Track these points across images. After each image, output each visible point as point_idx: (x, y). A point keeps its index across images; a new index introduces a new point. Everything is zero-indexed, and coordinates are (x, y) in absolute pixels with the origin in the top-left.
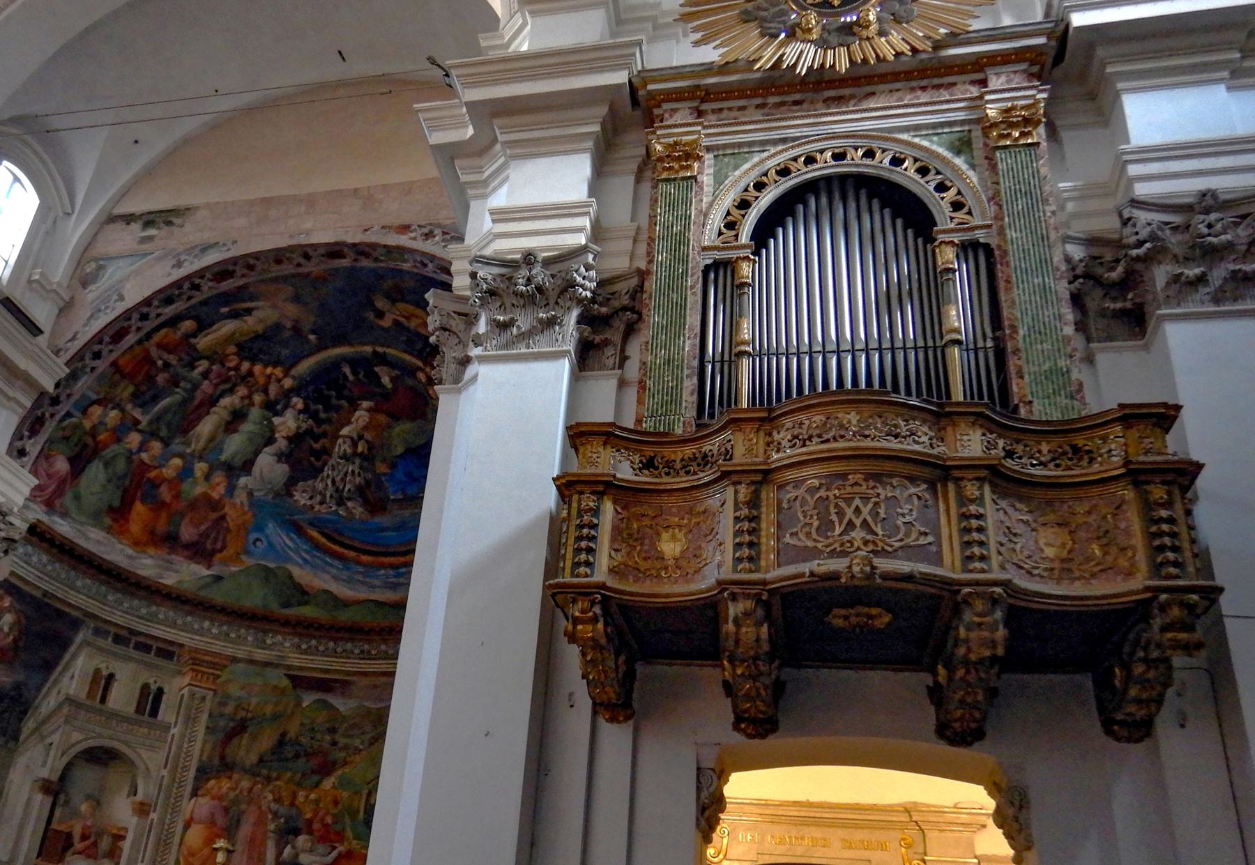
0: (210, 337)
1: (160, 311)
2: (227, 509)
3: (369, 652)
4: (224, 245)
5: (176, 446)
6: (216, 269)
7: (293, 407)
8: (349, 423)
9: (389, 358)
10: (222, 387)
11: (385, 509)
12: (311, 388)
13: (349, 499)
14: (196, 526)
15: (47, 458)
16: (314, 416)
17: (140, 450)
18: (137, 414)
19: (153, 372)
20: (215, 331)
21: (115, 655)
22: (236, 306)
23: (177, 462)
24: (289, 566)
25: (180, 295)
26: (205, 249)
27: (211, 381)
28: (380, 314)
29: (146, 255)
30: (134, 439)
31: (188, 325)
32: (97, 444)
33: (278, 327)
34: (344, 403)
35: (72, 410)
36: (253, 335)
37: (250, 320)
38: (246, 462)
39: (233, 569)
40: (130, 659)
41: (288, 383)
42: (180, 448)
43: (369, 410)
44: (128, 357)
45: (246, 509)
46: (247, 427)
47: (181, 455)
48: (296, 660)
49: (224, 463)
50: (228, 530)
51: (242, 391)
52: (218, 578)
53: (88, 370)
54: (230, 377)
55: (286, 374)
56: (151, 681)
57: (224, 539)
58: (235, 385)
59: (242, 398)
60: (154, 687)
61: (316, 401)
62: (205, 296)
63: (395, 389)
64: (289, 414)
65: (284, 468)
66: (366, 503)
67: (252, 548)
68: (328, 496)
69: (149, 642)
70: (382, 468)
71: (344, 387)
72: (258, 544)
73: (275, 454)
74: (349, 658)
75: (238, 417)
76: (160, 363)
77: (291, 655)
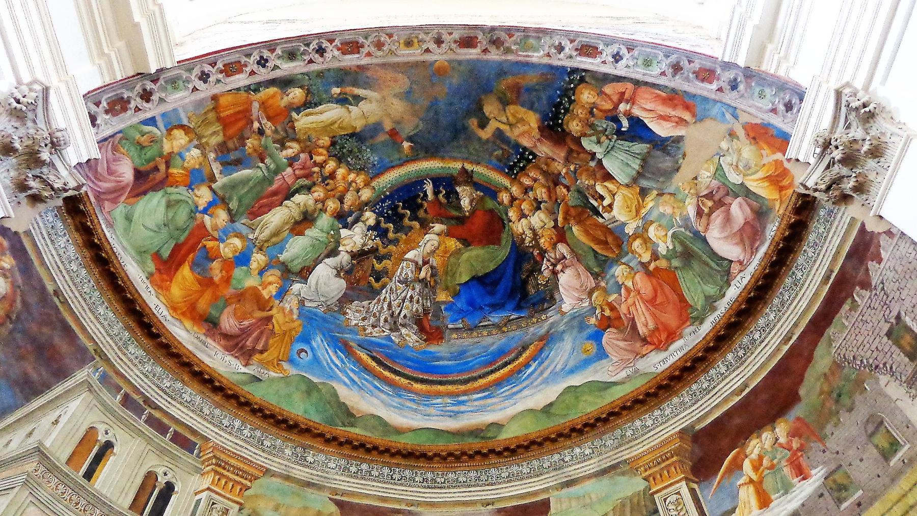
0: (311, 118)
1: (278, 63)
5: (241, 225)
6: (348, 37)
11: (442, 338)
12: (388, 203)
13: (404, 326)
14: (241, 319)
15: (115, 149)
16: (383, 234)
17: (205, 211)
18: (216, 168)
19: (247, 133)
21: (121, 420)
22: (348, 89)
23: (237, 242)
24: (335, 384)
25: (303, 54)
27: (294, 171)
30: (204, 195)
31: (296, 94)
32: (168, 175)
33: (375, 128)
34: (416, 224)
35: (159, 119)
38: (302, 269)
39: (273, 374)
40: (140, 433)
41: (366, 194)
42: (244, 230)
43: (438, 235)
45: (295, 317)
46: (312, 233)
51: (319, 193)
53: (191, 86)
55: (367, 184)
56: (160, 471)
58: (314, 184)
60: (162, 480)
61: (388, 219)
62: (325, 66)
63: (473, 212)
64: (359, 228)
65: (341, 284)
66: (422, 329)
67: (296, 357)
68: (382, 319)
69: (166, 421)
70: (442, 297)
72: (303, 355)
73: (335, 268)
75: (306, 219)
76: (256, 125)
77: (337, 477)
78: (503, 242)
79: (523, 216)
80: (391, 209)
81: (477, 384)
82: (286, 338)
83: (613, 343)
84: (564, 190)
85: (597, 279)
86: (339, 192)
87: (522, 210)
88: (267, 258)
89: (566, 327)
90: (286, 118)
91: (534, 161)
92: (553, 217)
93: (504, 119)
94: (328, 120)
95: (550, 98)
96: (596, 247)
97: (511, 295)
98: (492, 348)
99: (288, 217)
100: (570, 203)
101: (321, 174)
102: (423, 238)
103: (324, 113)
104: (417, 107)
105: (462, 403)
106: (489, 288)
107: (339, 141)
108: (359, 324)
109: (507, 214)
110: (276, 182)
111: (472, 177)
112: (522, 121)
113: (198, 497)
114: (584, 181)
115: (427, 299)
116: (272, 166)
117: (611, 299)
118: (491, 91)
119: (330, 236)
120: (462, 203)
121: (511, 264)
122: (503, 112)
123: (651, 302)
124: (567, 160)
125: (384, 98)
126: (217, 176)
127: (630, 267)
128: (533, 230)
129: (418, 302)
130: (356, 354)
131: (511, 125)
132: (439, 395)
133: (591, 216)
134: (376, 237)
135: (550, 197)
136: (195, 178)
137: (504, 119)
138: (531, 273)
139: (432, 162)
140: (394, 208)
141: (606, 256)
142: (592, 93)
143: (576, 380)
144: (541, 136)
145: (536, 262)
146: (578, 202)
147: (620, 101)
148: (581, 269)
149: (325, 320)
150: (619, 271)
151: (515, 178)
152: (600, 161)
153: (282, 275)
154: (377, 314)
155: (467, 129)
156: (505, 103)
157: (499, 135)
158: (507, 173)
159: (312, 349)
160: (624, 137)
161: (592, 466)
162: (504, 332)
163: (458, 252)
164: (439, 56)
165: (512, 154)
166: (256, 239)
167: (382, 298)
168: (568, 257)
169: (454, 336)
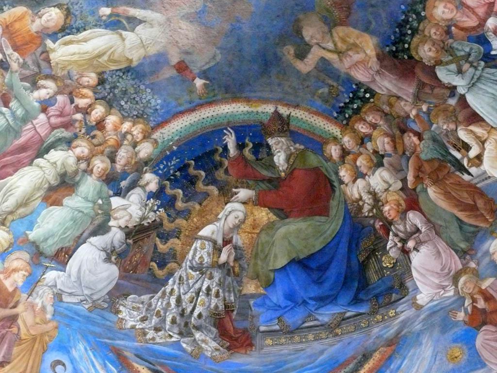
0: (73, 48)
2: (20, 309)
7: (143, 187)
9: (293, 125)
10: (62, 133)
11: (251, 345)
13: (198, 328)
16: (169, 203)
20: (78, 42)
22: (121, 9)
27: (49, 118)
34: (213, 190)
36: (123, 66)
41: (145, 150)
43: (244, 203)
45: (49, 316)
46: (75, 202)
49: (34, 244)
50: (18, 340)
51: (82, 148)
54: (76, 120)
55: (146, 137)
57: (10, 349)
58: (76, 137)
59: (79, 159)
61: (175, 182)
63: (291, 172)
64: (136, 196)
65: (112, 271)
68: (169, 319)
70: (251, 288)
71: (218, 166)
72: (59, 368)
73: (104, 250)
78: (333, 212)
79: (358, 175)
80: (180, 170)
82: (36, 346)
83: (492, 347)
84: (415, 139)
85: (465, 258)
86: (110, 146)
87: (357, 166)
88: (11, 236)
89: (423, 326)
90: (38, 47)
91: (372, 100)
92: (400, 176)
93: (330, 45)
94: (94, 50)
95: (391, 14)
96: (461, 215)
97: (346, 283)
98: (321, 358)
99: (40, 181)
100: (423, 156)
101: (86, 124)
102: (223, 209)
103: (90, 40)
104: (214, 32)
106: (315, 276)
107: (110, 79)
108: (137, 327)
109: (337, 173)
110: (25, 133)
111: (288, 124)
112: (355, 47)
114: (442, 125)
115: (229, 291)
116: (20, 112)
117: (486, 284)
118: (313, 9)
119: (97, 207)
120: (275, 158)
121: (345, 240)
122: (329, 36)
124: (418, 98)
125: (169, 20)
128: (374, 194)
129: (217, 295)
130: (133, 367)
131: (339, 53)
133: (453, 173)
134: (159, 207)
135: (395, 148)
137: (330, 45)
138: (374, 251)
139: (234, 105)
140: (184, 168)
141: (477, 227)
142: (449, 5)
144: (381, 67)
145: (379, 238)
146: (436, 155)
147: (489, 14)
148: (442, 245)
149: (88, 319)
151: (347, 124)
152: (462, 99)
153: (32, 258)
154: (162, 313)
155: (281, 59)
156: (331, 23)
157: (324, 67)
158: (336, 118)
159: (72, 361)
160: (493, 63)
162: (337, 335)
163: (270, 227)
165: (343, 93)
168: (423, 230)
169: (269, 342)
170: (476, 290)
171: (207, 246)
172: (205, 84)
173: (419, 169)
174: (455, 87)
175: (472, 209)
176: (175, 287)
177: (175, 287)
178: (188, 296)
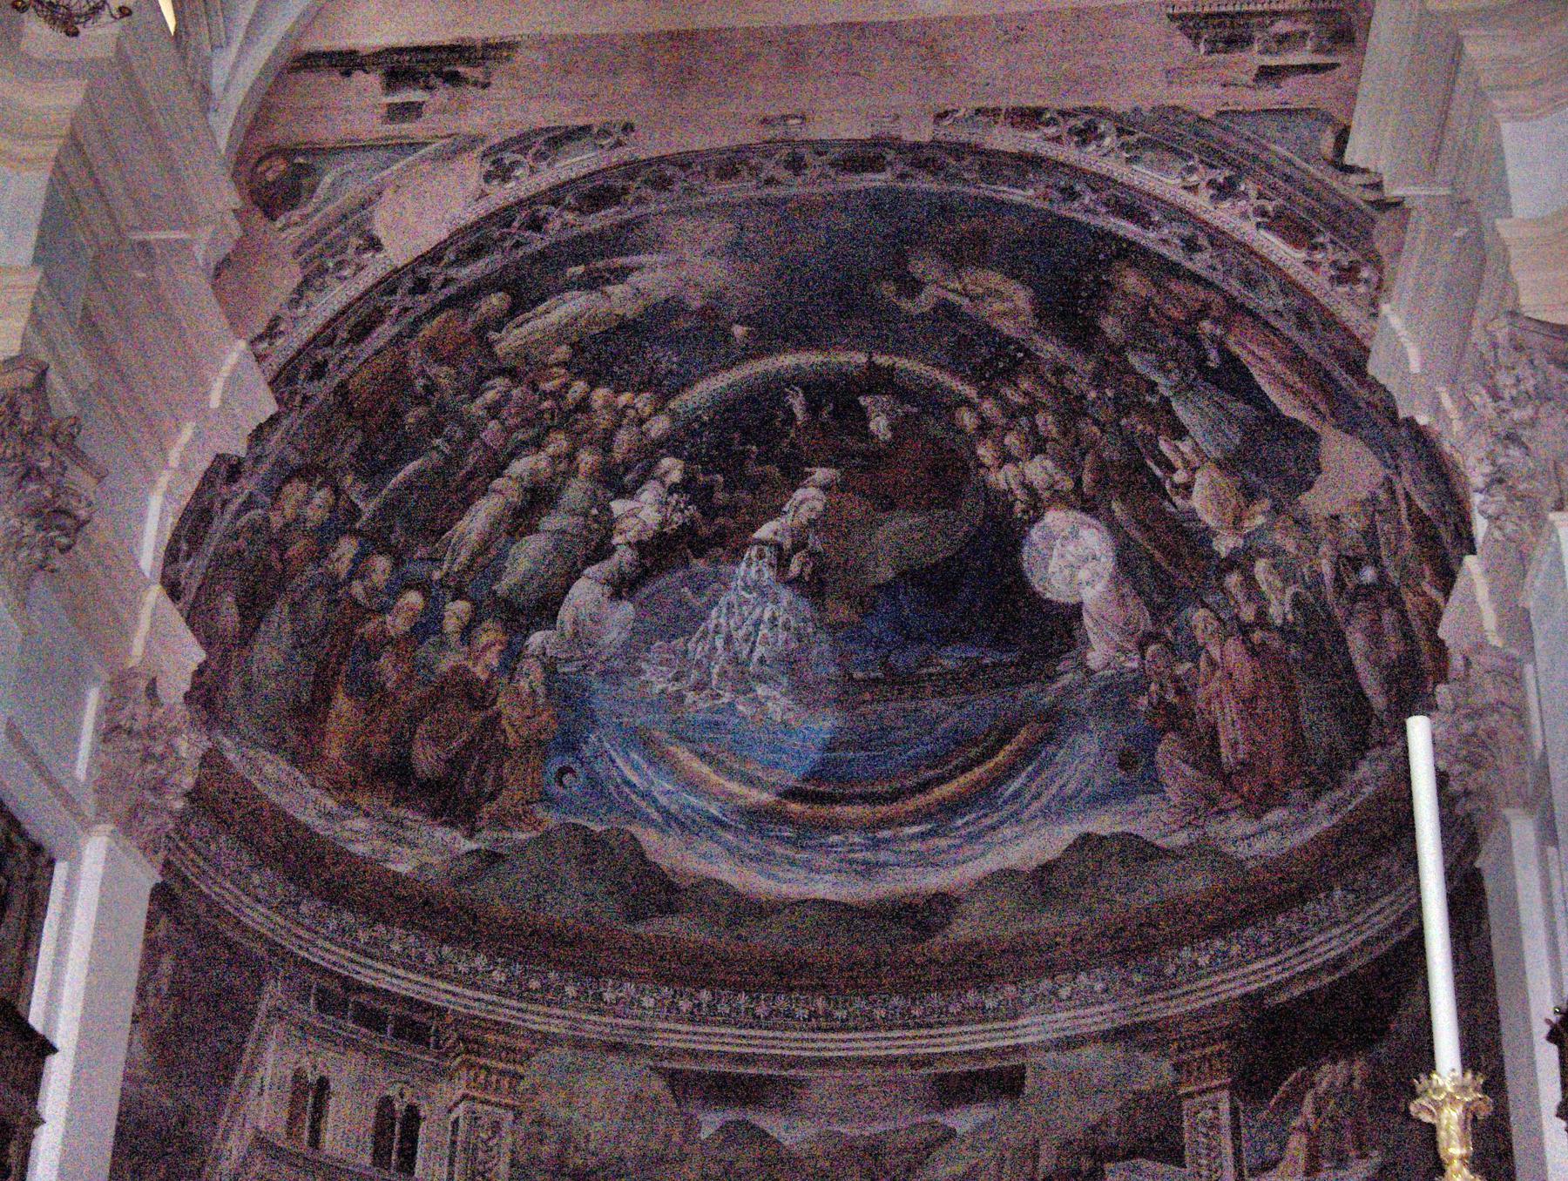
1: (452, 272)
2: (501, 701)
3: (828, 1015)
4: (605, 133)
8: (777, 512)
13: (760, 678)
23: (414, 598)
24: (636, 829)
25: (503, 238)
26: (560, 139)
27: (503, 424)
28: (912, 287)
29: (415, 146)
33: (670, 308)
34: (773, 471)
37: (617, 290)
39: (522, 836)
41: (659, 426)
43: (825, 488)
44: (366, 373)
45: (541, 701)
46: (552, 522)
47: (423, 587)
48: (676, 1035)
51: (558, 443)
52: (493, 858)
58: (548, 430)
59: (555, 458)
61: (710, 466)
64: (649, 494)
68: (715, 670)
72: (567, 778)
73: (608, 582)
74: (787, 1028)
75: (539, 498)
79: (1006, 458)
81: (912, 804)
84: (1095, 429)
105: (877, 844)
113: (453, 1116)
114: (1137, 424)
116: (459, 435)
117: (1182, 668)
120: (872, 426)
123: (1249, 703)
124: (1098, 380)
126: (361, 505)
127: (1219, 619)
129: (787, 627)
132: (834, 826)
135: (1065, 434)
136: (325, 536)
143: (1104, 823)
150: (1199, 616)
152: (1166, 401)
161: (1096, 1019)
164: (795, 188)
166: (447, 574)
167: (712, 627)
170: (1168, 672)
171: (768, 554)
172: (750, 333)
173: (1102, 468)
174: (1156, 384)
175: (1174, 556)
176: (722, 620)
177: (722, 620)
178: (741, 633)
